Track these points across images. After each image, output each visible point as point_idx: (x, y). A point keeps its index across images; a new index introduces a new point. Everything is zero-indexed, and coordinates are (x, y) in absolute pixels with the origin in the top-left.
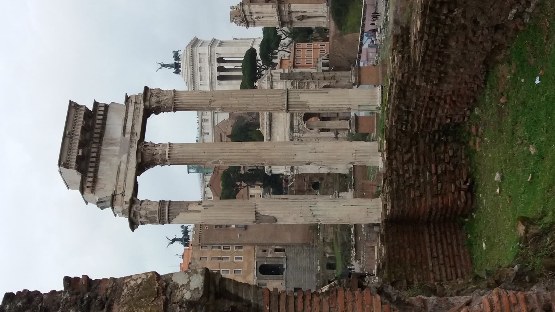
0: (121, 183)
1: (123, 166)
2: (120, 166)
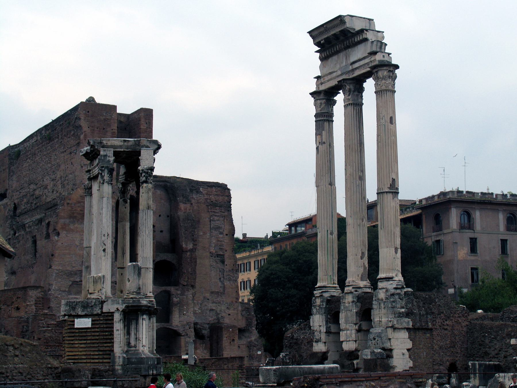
0: (326, 78)
1: (334, 75)
2: (334, 72)
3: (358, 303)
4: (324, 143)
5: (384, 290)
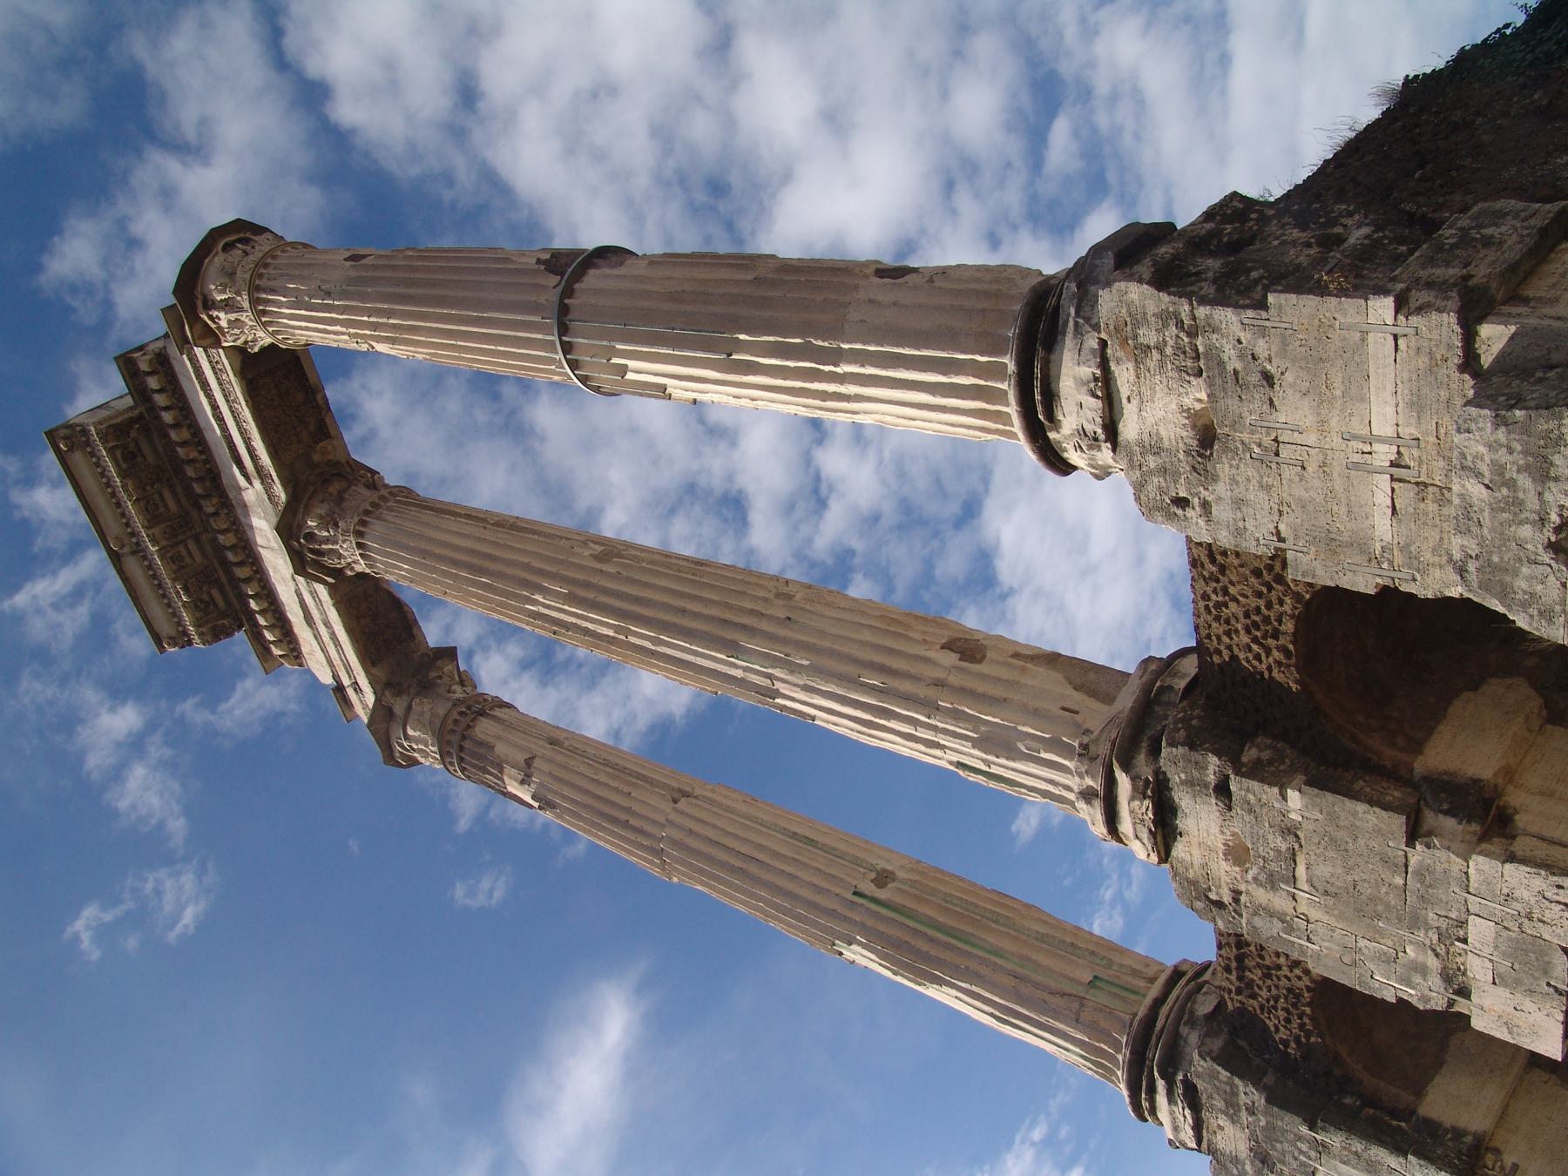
3: (1250, 754)
4: (529, 762)
5: (1124, 375)
